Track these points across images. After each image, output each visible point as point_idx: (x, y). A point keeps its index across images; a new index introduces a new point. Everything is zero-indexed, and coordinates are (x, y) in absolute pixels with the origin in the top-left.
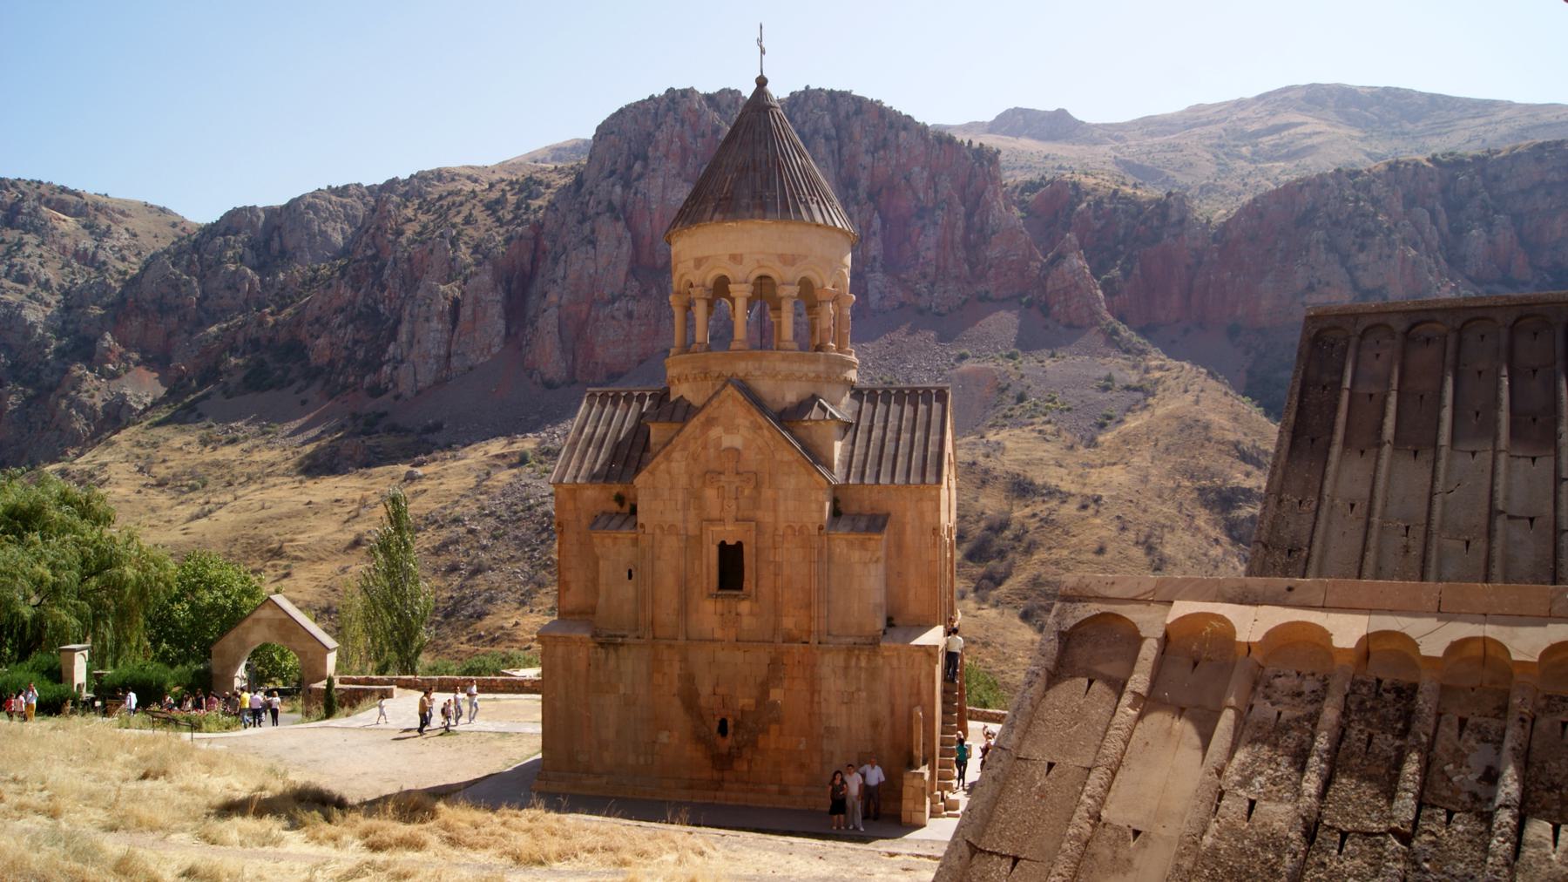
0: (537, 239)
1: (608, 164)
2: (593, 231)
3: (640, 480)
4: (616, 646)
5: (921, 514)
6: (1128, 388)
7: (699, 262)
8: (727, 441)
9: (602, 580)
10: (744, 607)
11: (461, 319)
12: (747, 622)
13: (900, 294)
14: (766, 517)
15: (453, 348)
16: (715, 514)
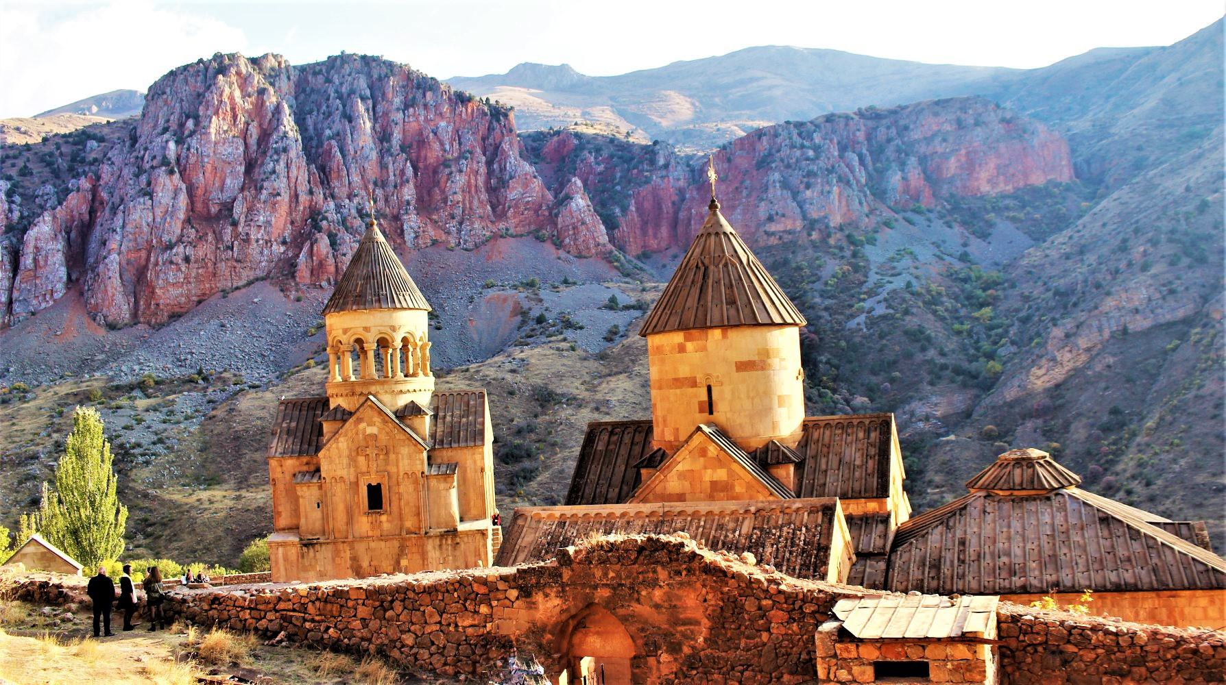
0: (94, 190)
1: (161, 122)
2: (149, 184)
3: (321, 454)
4: (313, 545)
5: (475, 462)
6: (627, 308)
7: (345, 331)
8: (370, 430)
9: (302, 509)
10: (384, 518)
11: (22, 267)
12: (386, 526)
13: (432, 233)
14: (393, 469)
15: (15, 294)
16: (364, 469)
